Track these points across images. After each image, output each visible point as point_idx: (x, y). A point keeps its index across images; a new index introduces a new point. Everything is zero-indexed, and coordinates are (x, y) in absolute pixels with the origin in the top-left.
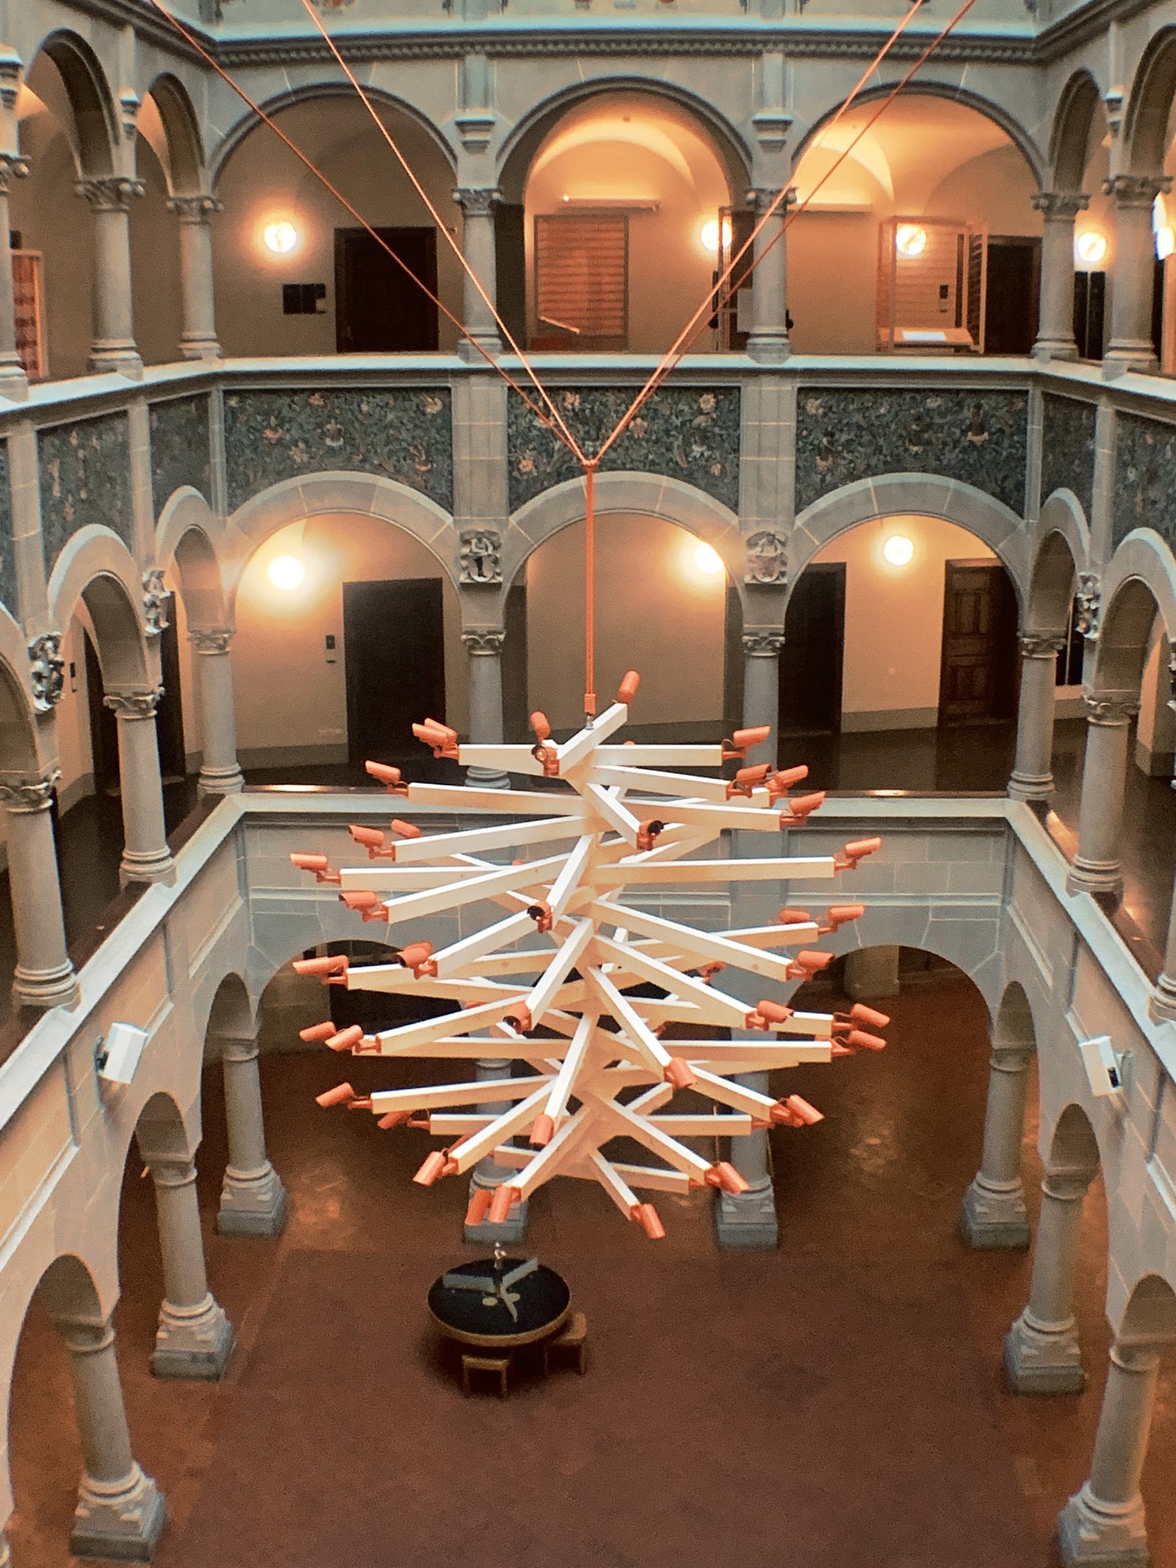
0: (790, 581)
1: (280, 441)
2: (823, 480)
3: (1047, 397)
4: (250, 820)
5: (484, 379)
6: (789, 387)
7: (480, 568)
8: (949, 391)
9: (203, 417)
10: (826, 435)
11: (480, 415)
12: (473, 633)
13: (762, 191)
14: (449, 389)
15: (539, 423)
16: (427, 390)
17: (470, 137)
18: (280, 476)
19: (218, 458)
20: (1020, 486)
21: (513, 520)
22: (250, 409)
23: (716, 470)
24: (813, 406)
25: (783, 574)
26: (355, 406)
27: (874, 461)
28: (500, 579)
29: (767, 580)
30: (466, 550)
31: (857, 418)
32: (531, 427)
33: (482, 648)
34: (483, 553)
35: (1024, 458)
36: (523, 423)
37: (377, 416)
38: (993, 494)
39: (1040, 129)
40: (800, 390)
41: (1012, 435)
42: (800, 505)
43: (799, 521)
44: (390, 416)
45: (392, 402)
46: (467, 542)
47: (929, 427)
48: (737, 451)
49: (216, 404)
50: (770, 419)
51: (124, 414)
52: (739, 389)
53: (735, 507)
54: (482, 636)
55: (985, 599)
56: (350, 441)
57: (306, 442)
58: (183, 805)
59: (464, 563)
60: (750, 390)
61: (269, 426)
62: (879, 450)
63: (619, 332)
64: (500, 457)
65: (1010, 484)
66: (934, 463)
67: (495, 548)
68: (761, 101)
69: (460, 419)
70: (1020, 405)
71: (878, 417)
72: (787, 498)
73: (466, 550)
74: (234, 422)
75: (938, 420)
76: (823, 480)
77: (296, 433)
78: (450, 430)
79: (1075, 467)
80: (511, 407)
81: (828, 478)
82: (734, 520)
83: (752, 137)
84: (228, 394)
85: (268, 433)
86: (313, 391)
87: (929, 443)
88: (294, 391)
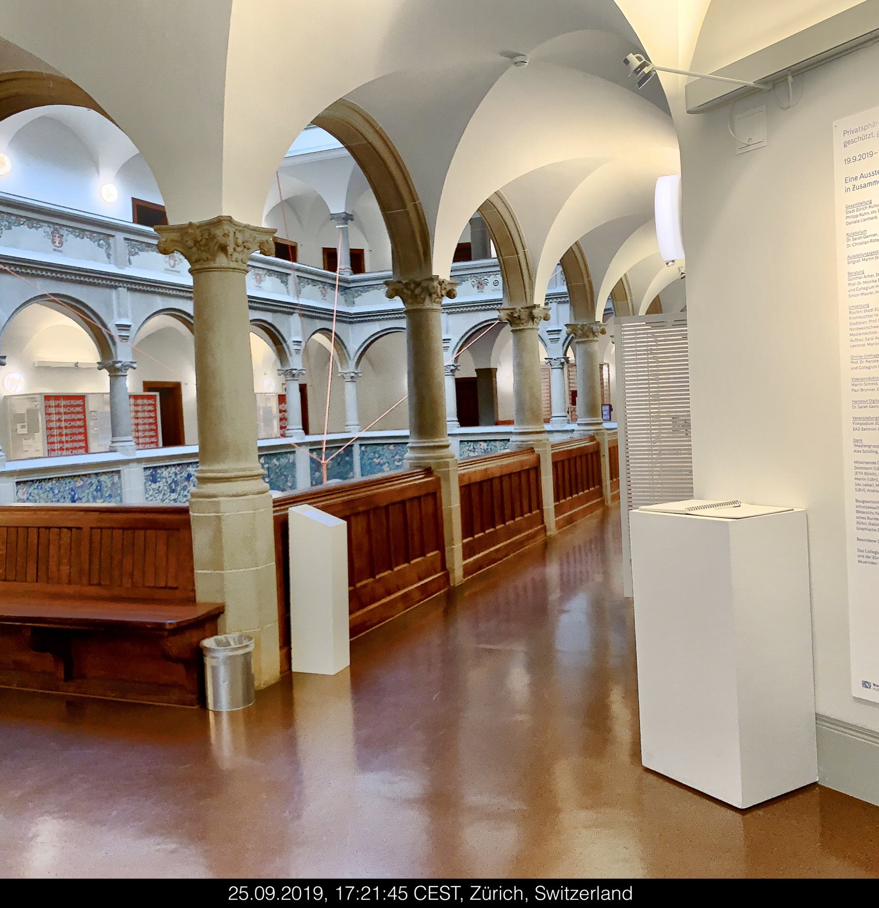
49: (356, 450)
51: (294, 452)
77: (385, 460)
85: (375, 460)
86: (391, 444)
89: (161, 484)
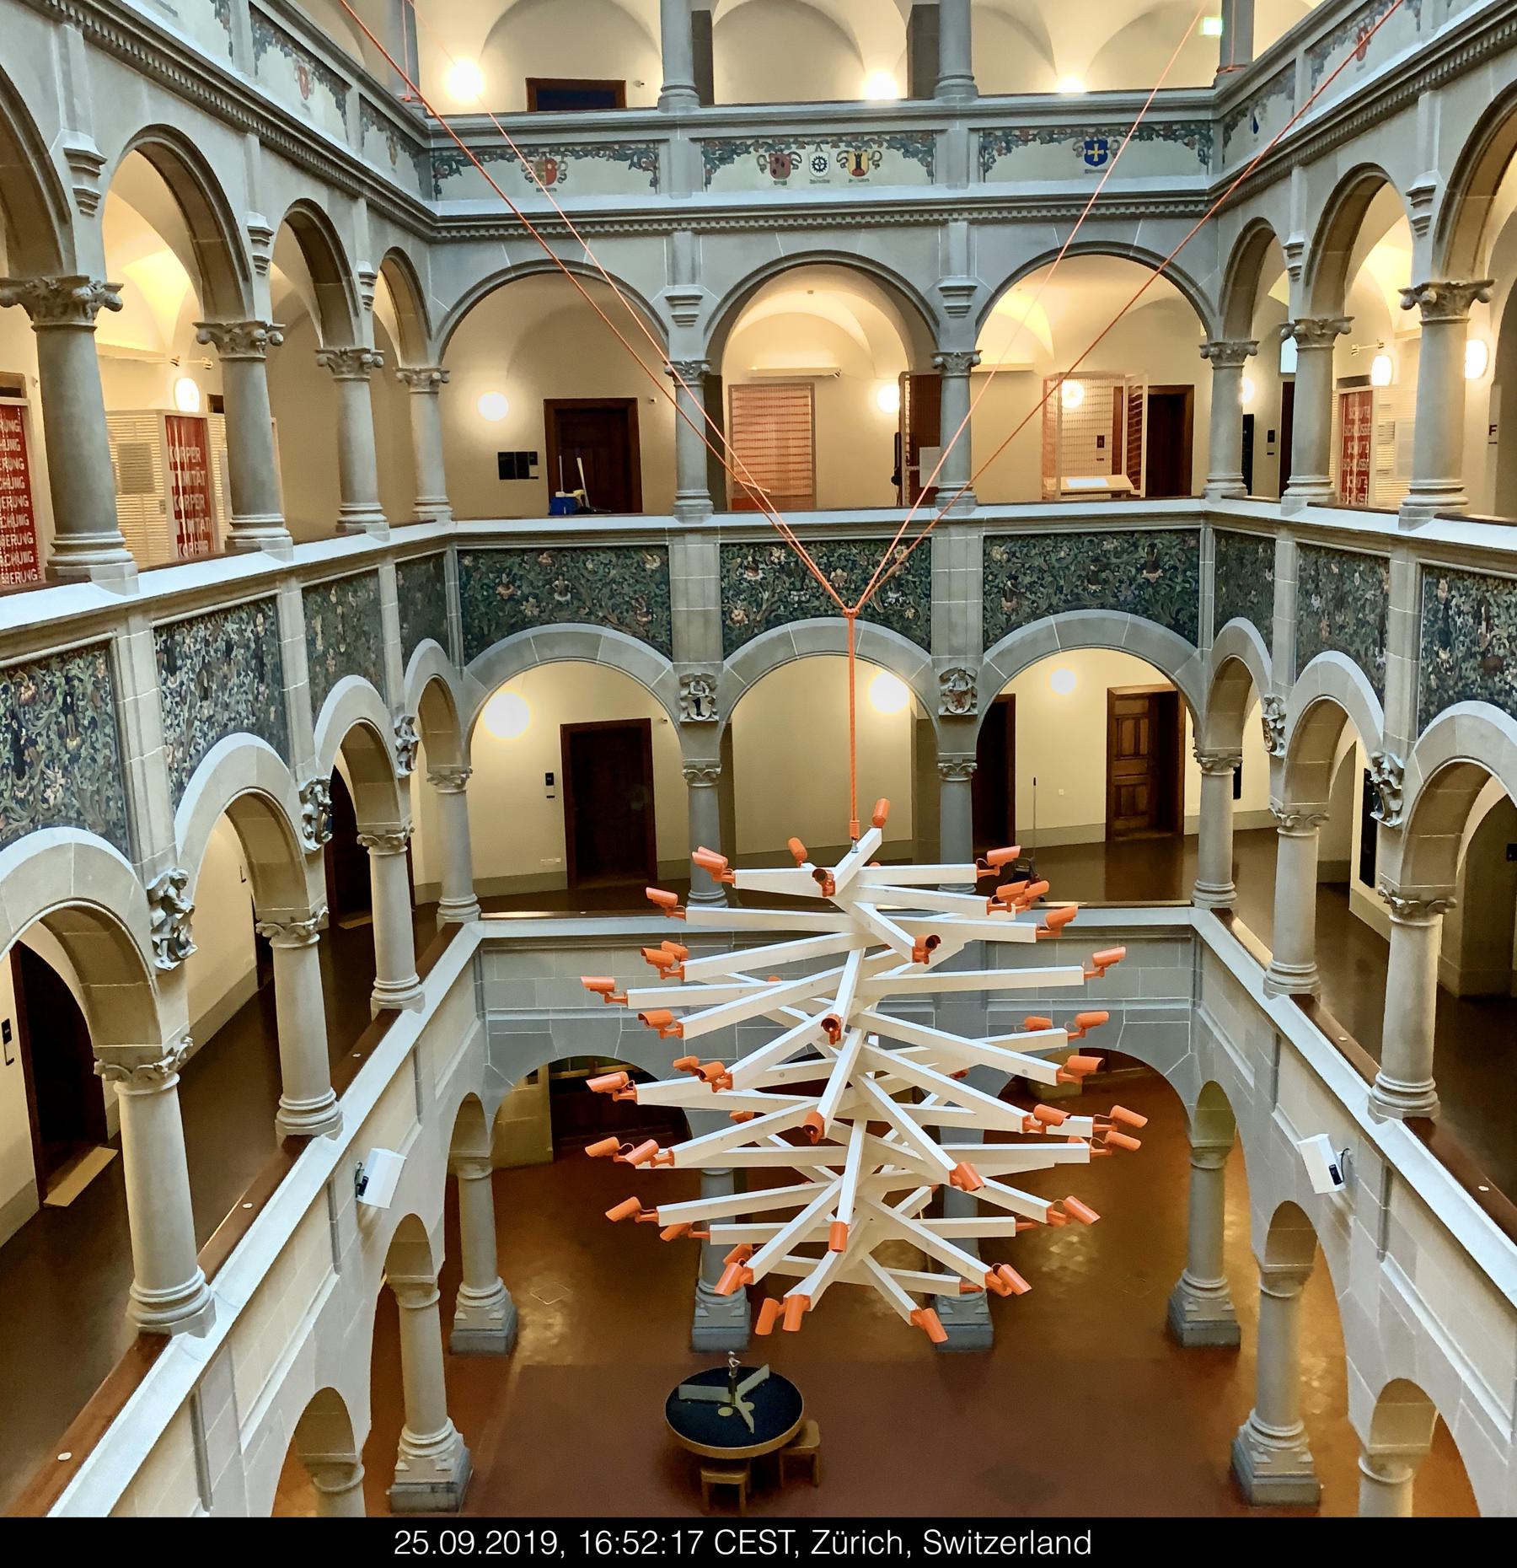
0: (981, 711)
1: (511, 597)
2: (1008, 619)
3: (1216, 532)
4: (489, 946)
5: (698, 537)
6: (976, 536)
7: (698, 707)
8: (1124, 533)
9: (439, 576)
10: (1010, 578)
11: (695, 571)
12: (694, 767)
13: (949, 354)
14: (666, 547)
15: (749, 575)
16: (647, 548)
17: (679, 311)
18: (513, 629)
19: (454, 613)
20: (1194, 617)
21: (727, 664)
22: (483, 569)
23: (910, 614)
24: (998, 553)
25: (974, 706)
26: (580, 564)
27: (1055, 601)
28: (717, 718)
29: (960, 711)
30: (685, 692)
31: (1039, 562)
32: (741, 580)
33: (701, 781)
34: (701, 694)
35: (1197, 591)
36: (734, 577)
37: (601, 572)
38: (1168, 626)
39: (1211, 281)
40: (986, 537)
41: (1185, 571)
42: (987, 642)
43: (988, 657)
44: (613, 572)
45: (614, 560)
46: (687, 685)
47: (1106, 567)
48: (929, 596)
50: (959, 568)
52: (929, 539)
53: (928, 648)
54: (701, 770)
55: (1144, 724)
56: (576, 596)
57: (536, 597)
58: (432, 932)
59: (684, 704)
60: (939, 540)
61: (501, 583)
62: (1060, 589)
63: (809, 491)
64: (714, 608)
65: (1183, 617)
66: (1112, 600)
67: (712, 690)
68: (948, 271)
69: (677, 574)
70: (1193, 543)
71: (1058, 560)
72: (976, 638)
73: (685, 692)
74: (468, 580)
75: (1114, 560)
76: (1008, 619)
77: (526, 589)
78: (668, 583)
79: (1251, 597)
80: (723, 562)
81: (1013, 617)
82: (928, 658)
83: (941, 303)
84: (462, 554)
85: (500, 589)
86: (542, 551)
87: (1106, 581)
88: (524, 551)
89: (182, 676)
